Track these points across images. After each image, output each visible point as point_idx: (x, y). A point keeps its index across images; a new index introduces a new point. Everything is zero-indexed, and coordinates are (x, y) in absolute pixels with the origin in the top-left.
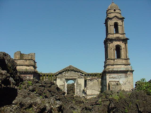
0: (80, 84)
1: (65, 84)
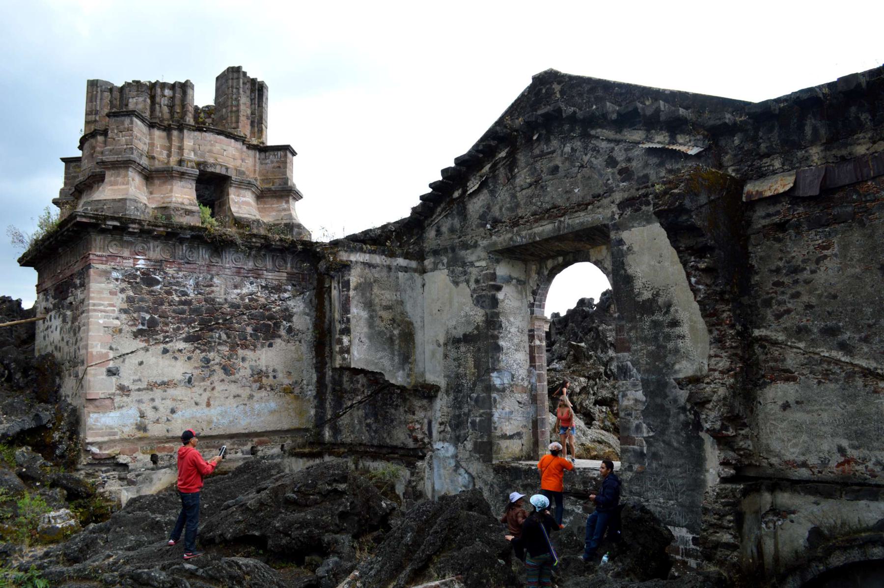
0: (649, 307)
1: (493, 323)
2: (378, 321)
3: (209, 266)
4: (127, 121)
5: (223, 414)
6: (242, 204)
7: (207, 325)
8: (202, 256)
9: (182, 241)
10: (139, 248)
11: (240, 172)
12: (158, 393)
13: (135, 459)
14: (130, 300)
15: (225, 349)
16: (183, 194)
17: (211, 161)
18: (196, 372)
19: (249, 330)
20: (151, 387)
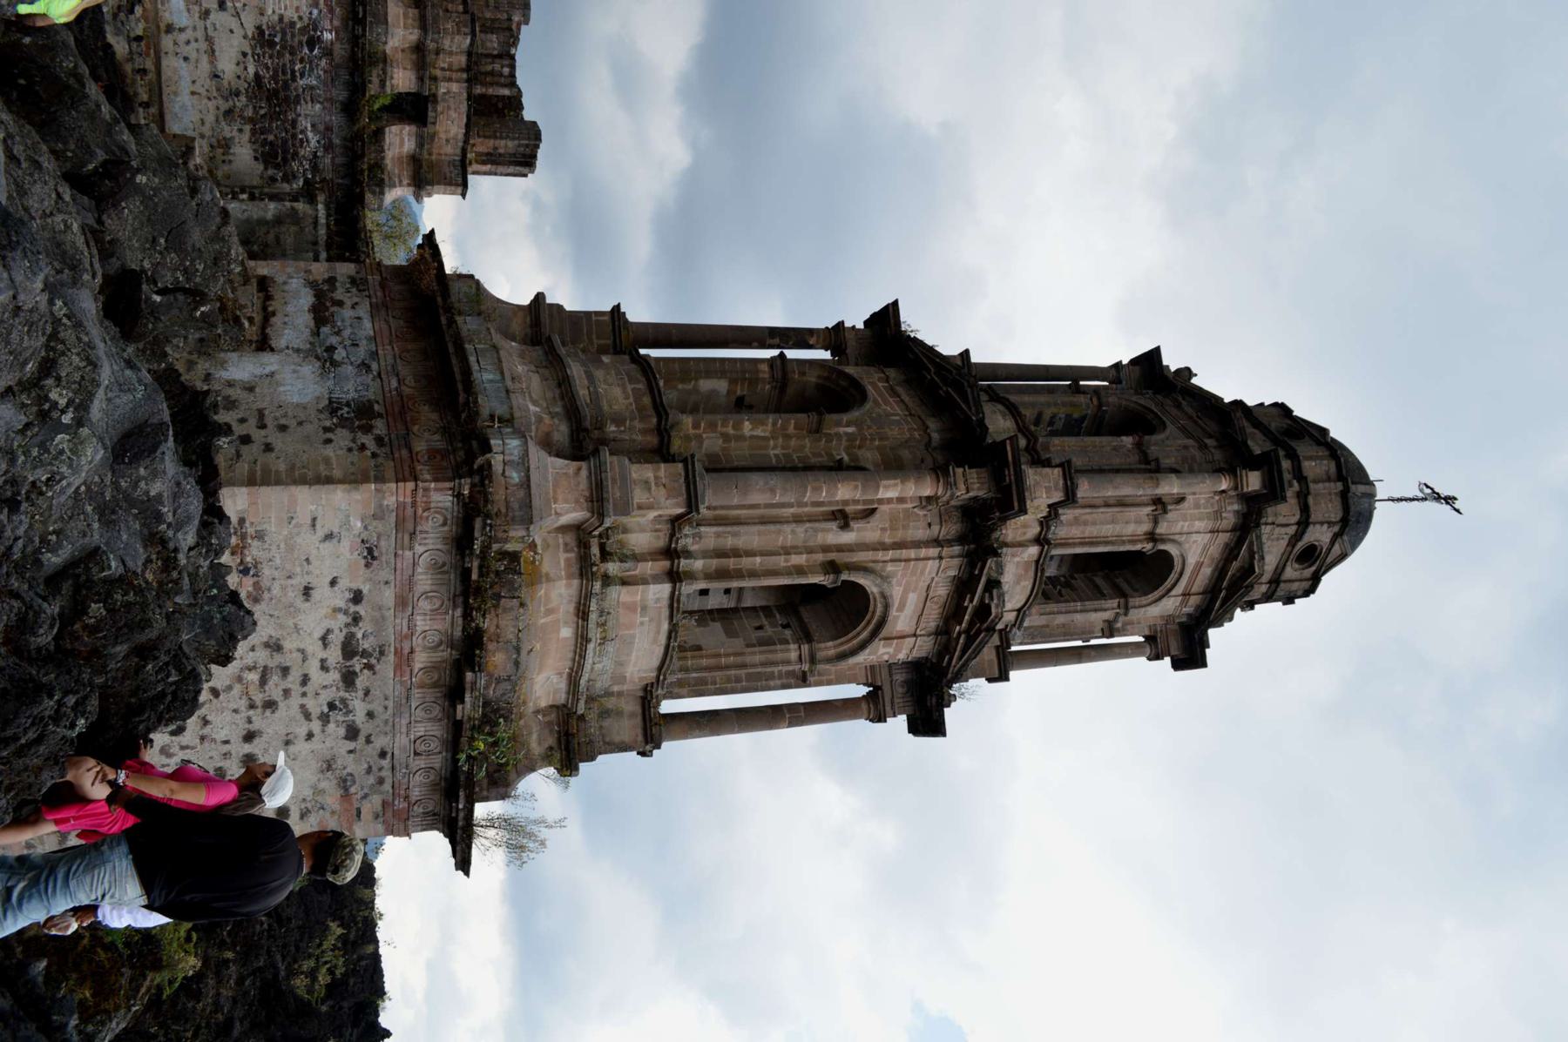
2: (264, 229)
3: (330, 100)
4: (467, 30)
5: (183, 107)
6: (399, 140)
7: (270, 98)
8: (341, 94)
9: (352, 75)
10: (342, 35)
11: (433, 136)
12: (203, 46)
13: (138, 20)
14: (292, 24)
15: (249, 112)
16: (402, 79)
17: (439, 109)
18: (225, 83)
19: (271, 138)
20: (208, 39)
